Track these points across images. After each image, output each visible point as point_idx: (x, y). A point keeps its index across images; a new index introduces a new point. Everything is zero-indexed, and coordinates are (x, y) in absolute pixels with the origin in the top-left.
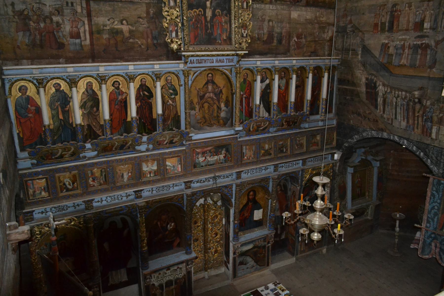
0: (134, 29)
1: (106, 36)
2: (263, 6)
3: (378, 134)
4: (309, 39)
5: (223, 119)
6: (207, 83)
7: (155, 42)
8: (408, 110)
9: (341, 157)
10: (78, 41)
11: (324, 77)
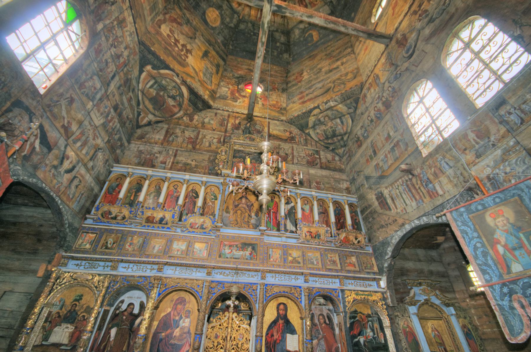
1: (180, 165)
3: (402, 232)
4: (327, 186)
5: (252, 224)
7: (210, 172)
8: (410, 190)
9: (388, 282)
10: (164, 165)
11: (345, 209)
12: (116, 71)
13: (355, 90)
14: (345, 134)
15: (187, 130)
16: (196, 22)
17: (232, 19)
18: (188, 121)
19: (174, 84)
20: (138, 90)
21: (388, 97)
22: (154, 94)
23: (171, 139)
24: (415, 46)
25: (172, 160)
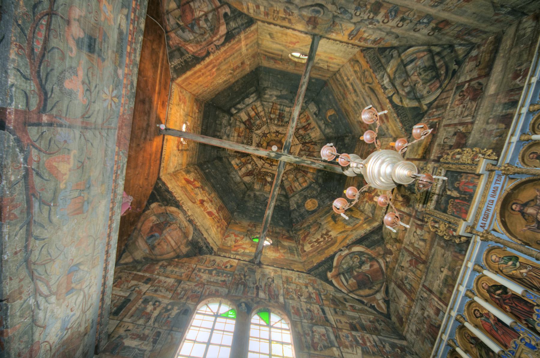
0: (448, 265)
1: (445, 291)
2: (473, 132)
6: (523, 214)
12: (320, 306)
13: (370, 57)
14: (430, 51)
15: (401, 262)
16: (311, 220)
17: (314, 189)
18: (391, 257)
19: (348, 257)
20: (347, 295)
21: (367, 11)
22: (355, 281)
23: (408, 286)
24: (312, 6)
25: (436, 299)
